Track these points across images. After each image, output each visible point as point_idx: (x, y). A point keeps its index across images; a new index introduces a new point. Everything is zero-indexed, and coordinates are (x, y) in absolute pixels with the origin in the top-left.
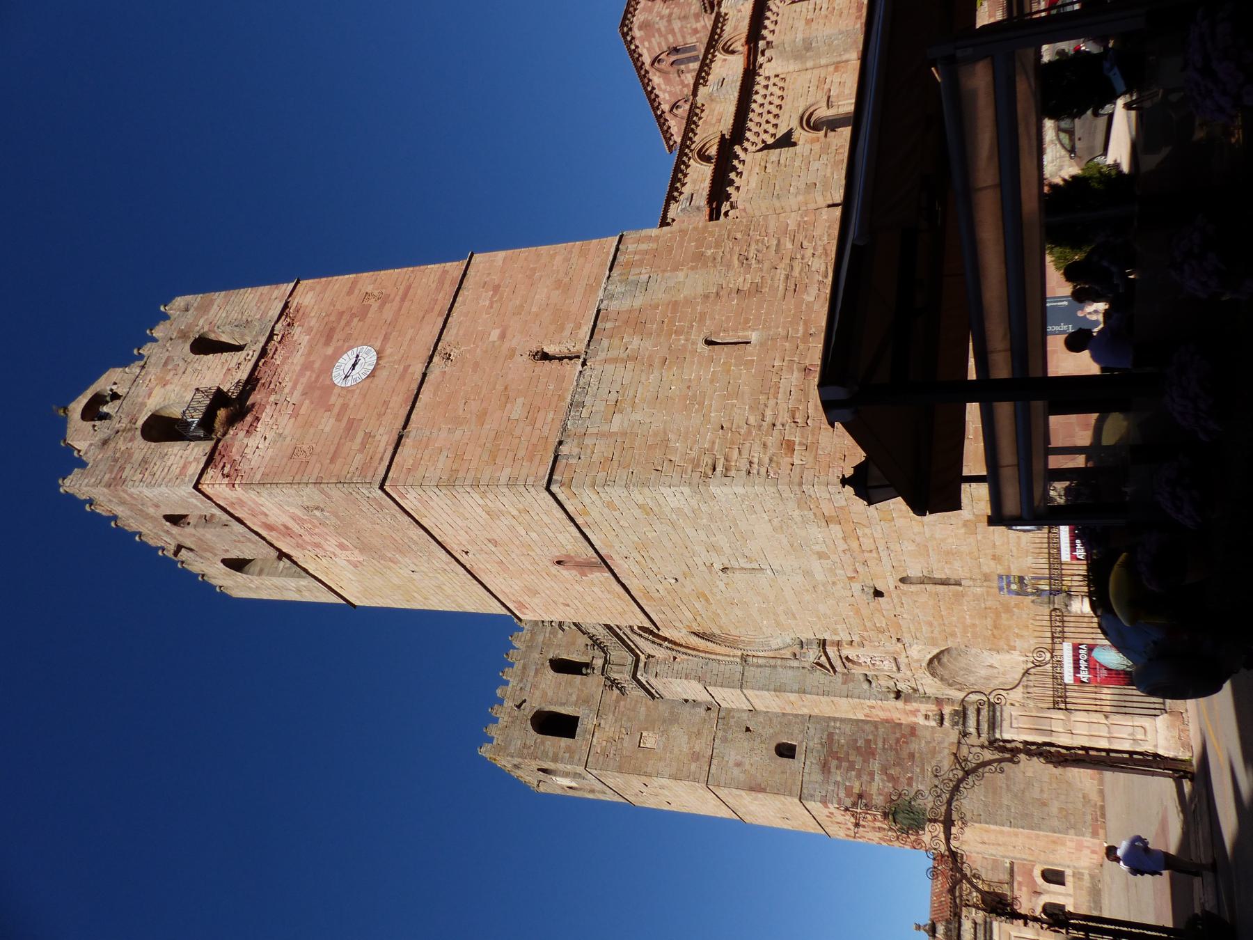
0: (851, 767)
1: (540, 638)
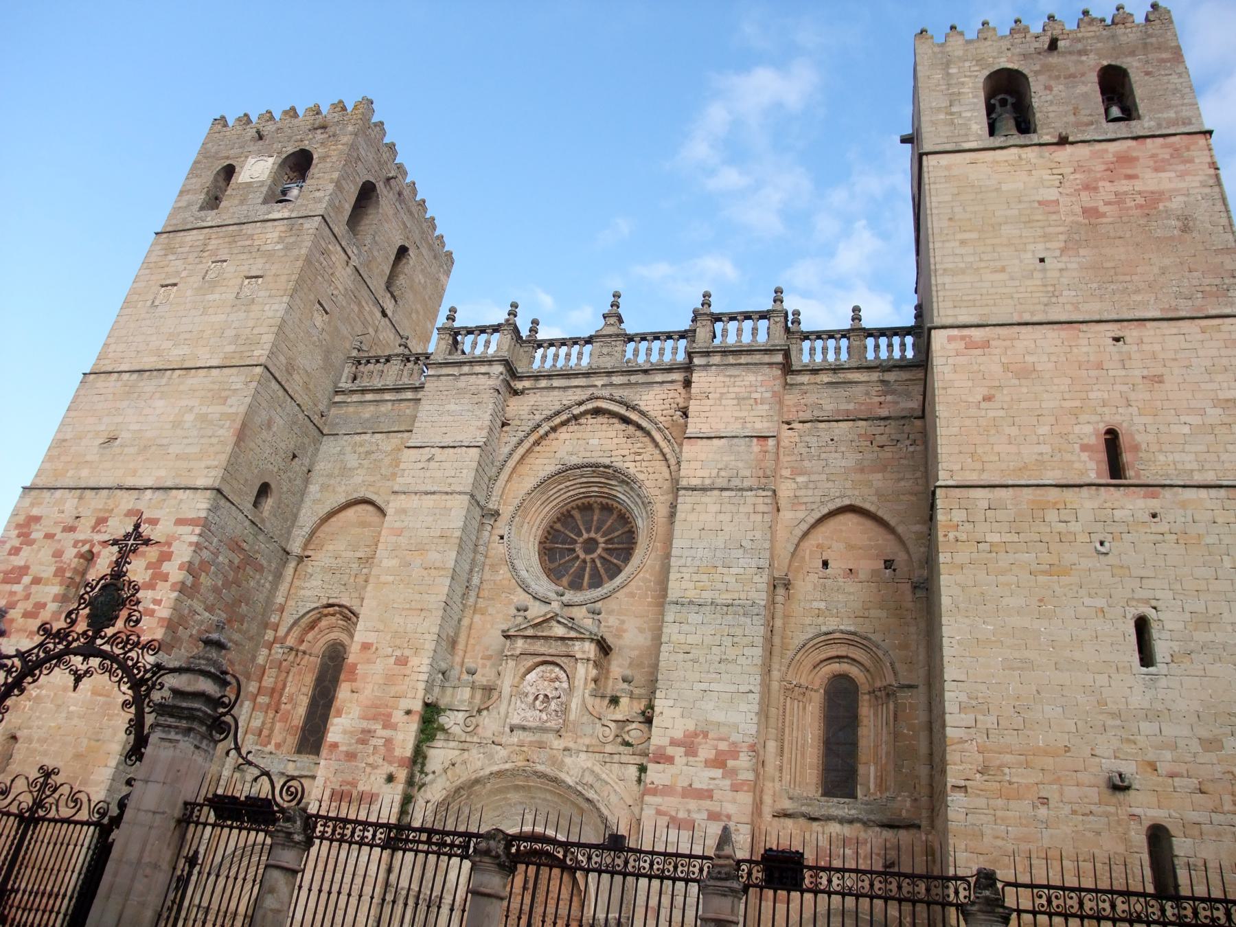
0: (227, 584)
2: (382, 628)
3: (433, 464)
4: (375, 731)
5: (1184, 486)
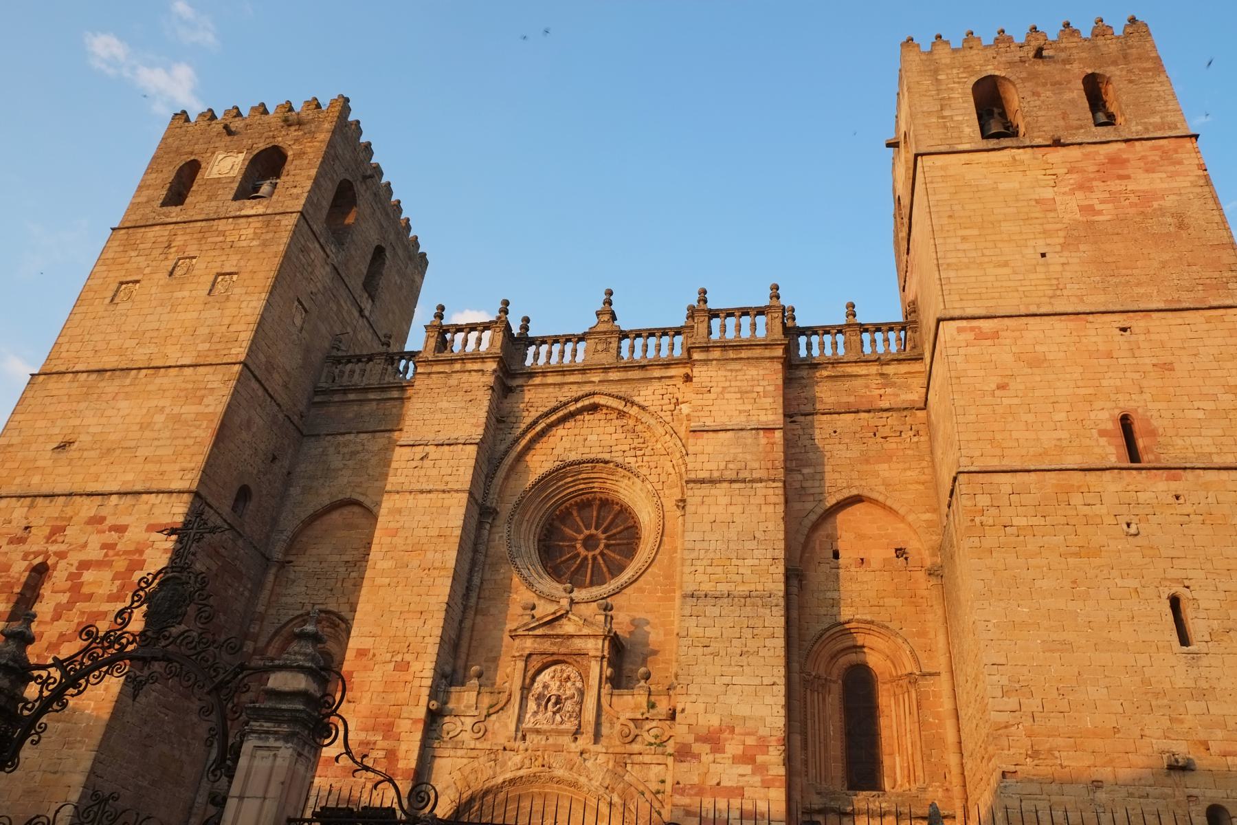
1: (400, 252)
2: (379, 632)
3: (427, 463)
4: (375, 743)
5: (1204, 469)
